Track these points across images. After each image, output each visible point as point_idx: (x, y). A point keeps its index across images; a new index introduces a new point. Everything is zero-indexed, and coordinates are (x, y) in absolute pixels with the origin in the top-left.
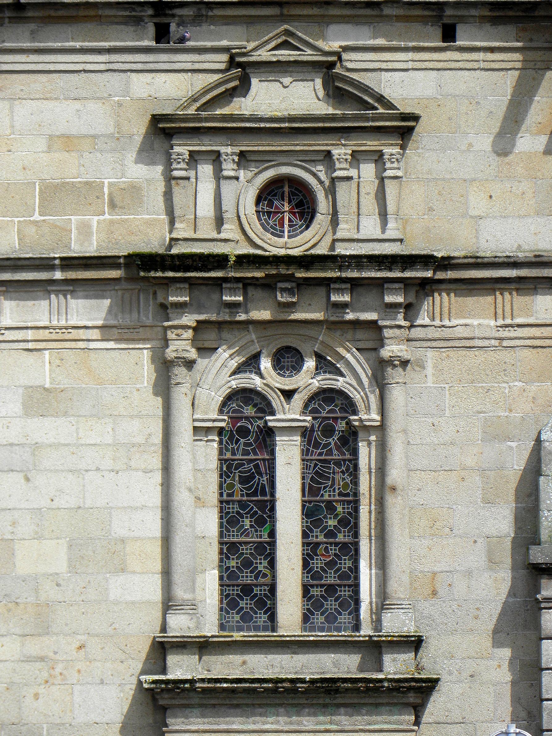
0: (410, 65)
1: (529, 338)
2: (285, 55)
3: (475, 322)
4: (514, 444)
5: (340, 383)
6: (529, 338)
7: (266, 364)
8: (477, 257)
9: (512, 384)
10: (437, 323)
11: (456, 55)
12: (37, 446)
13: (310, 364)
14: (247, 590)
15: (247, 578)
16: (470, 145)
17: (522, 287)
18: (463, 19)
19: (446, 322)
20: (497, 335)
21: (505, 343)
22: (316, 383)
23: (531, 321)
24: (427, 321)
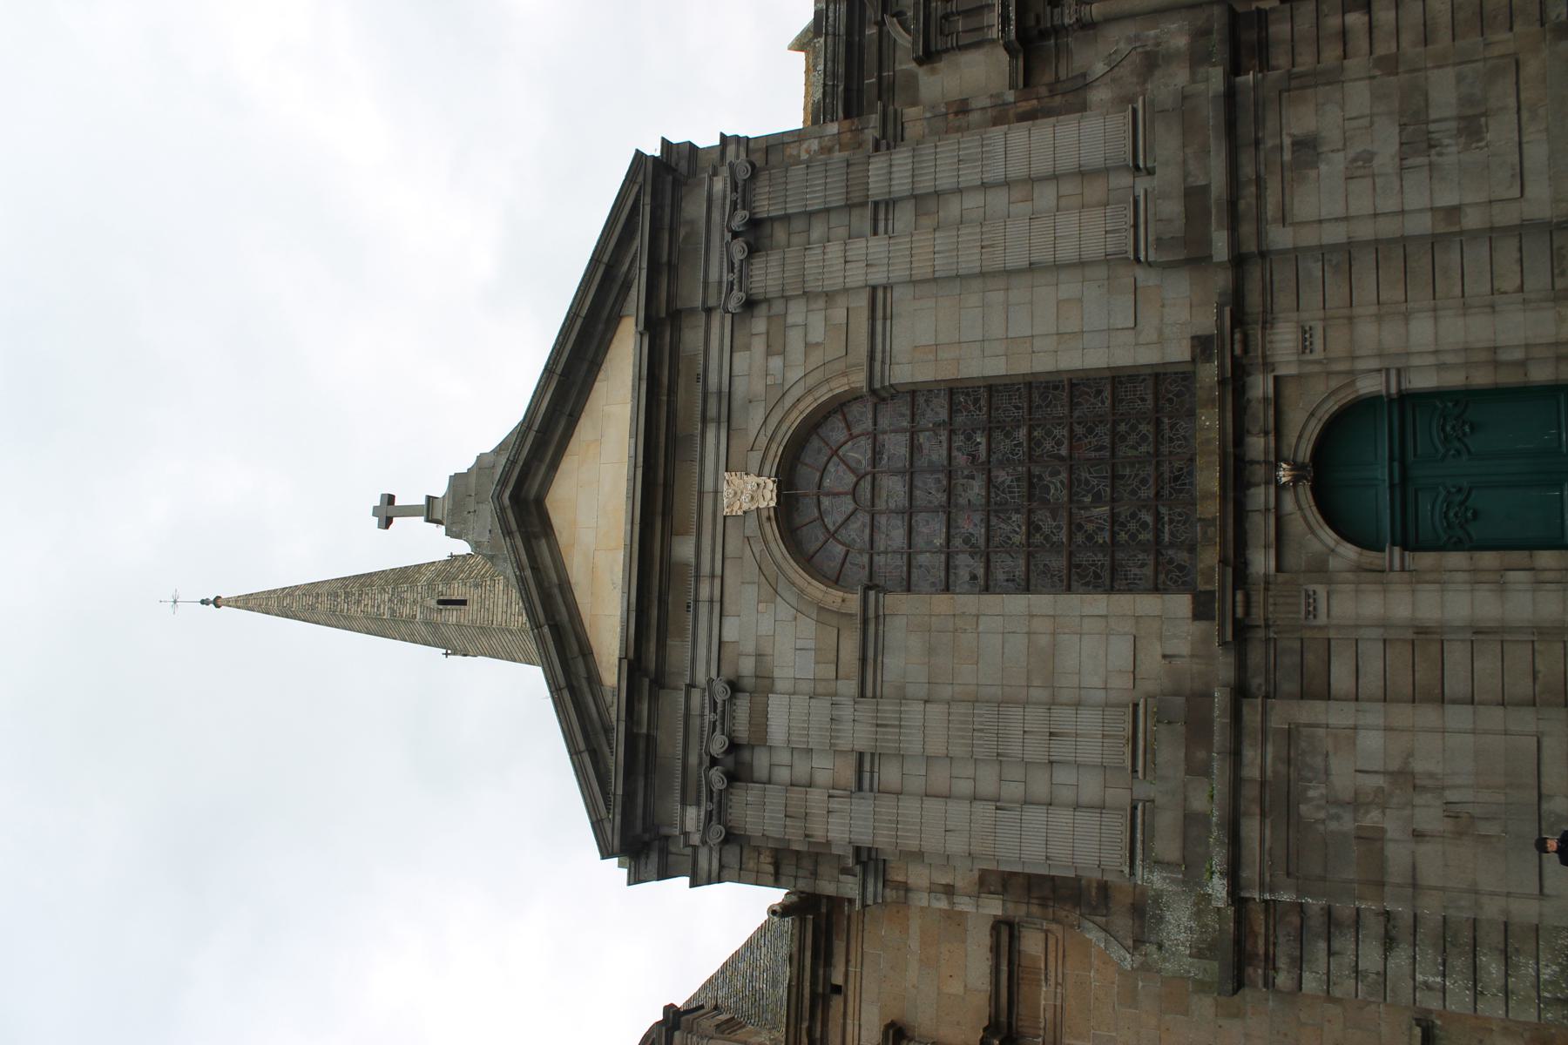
0: (856, 1022)
1: (1057, 962)
3: (1043, 1002)
4: (1140, 984)
6: (1057, 962)
8: (990, 996)
9: (1092, 980)
10: (1042, 1032)
11: (851, 987)
16: (913, 986)
17: (1017, 962)
18: (827, 978)
19: (1042, 1025)
20: (1053, 986)
21: (1060, 981)
23: (1043, 958)
24: (1040, 1040)
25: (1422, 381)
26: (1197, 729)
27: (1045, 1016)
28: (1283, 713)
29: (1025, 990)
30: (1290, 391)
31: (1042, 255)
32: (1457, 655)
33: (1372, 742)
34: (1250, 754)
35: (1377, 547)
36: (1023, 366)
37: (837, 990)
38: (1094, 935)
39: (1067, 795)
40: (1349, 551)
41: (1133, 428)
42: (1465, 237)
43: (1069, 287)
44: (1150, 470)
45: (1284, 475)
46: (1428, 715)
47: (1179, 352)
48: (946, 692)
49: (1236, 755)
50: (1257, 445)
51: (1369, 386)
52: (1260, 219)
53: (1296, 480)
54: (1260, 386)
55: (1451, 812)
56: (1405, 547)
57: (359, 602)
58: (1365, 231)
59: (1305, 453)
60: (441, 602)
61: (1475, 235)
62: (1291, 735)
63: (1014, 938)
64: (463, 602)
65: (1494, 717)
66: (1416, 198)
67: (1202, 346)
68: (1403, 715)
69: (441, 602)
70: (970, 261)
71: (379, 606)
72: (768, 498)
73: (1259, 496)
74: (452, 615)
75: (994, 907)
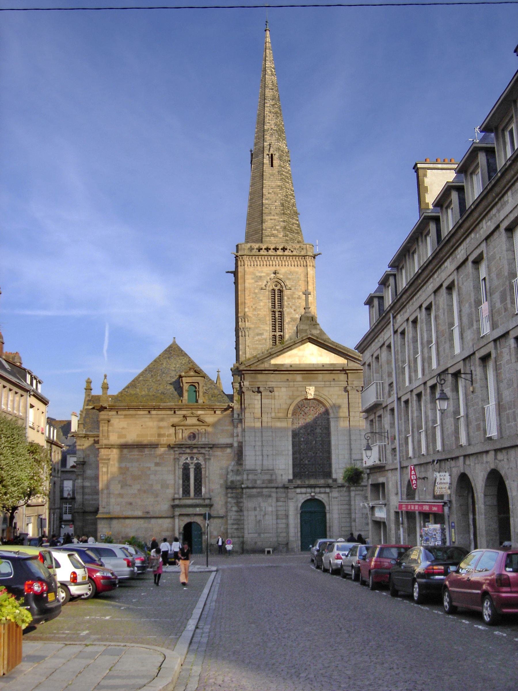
2: (192, 415)
5: (199, 462)
7: (189, 459)
12: (156, 471)
13: (195, 459)
14: (186, 491)
15: (186, 489)
22: (196, 462)
25: (328, 516)
26: (270, 481)
27: (216, 453)
28: (274, 495)
29: (220, 449)
30: (327, 495)
31: (353, 452)
32: (284, 521)
33: (270, 509)
34: (267, 490)
35: (301, 509)
36: (333, 448)
37: (215, 412)
38: (233, 463)
39: (257, 458)
40: (300, 505)
41: (321, 467)
42: (351, 522)
43: (347, 456)
44: (314, 470)
45: (313, 494)
46: (275, 517)
47: (334, 476)
48: (274, 435)
49: (267, 488)
50: (317, 490)
51: (327, 508)
52: (356, 490)
53: (312, 496)
54: (328, 490)
55: (260, 521)
56: (301, 513)
57: (270, 112)
58: (353, 507)
59: (316, 497)
60: (272, 155)
61: (351, 524)
62: (270, 496)
63: (229, 447)
64: (272, 166)
65: (275, 527)
66: (357, 516)
67: (335, 480)
68: (275, 513)
69: (272, 155)
70: (353, 438)
71: (269, 123)
72: (309, 397)
73: (309, 490)
74: (266, 161)
75: (236, 445)
